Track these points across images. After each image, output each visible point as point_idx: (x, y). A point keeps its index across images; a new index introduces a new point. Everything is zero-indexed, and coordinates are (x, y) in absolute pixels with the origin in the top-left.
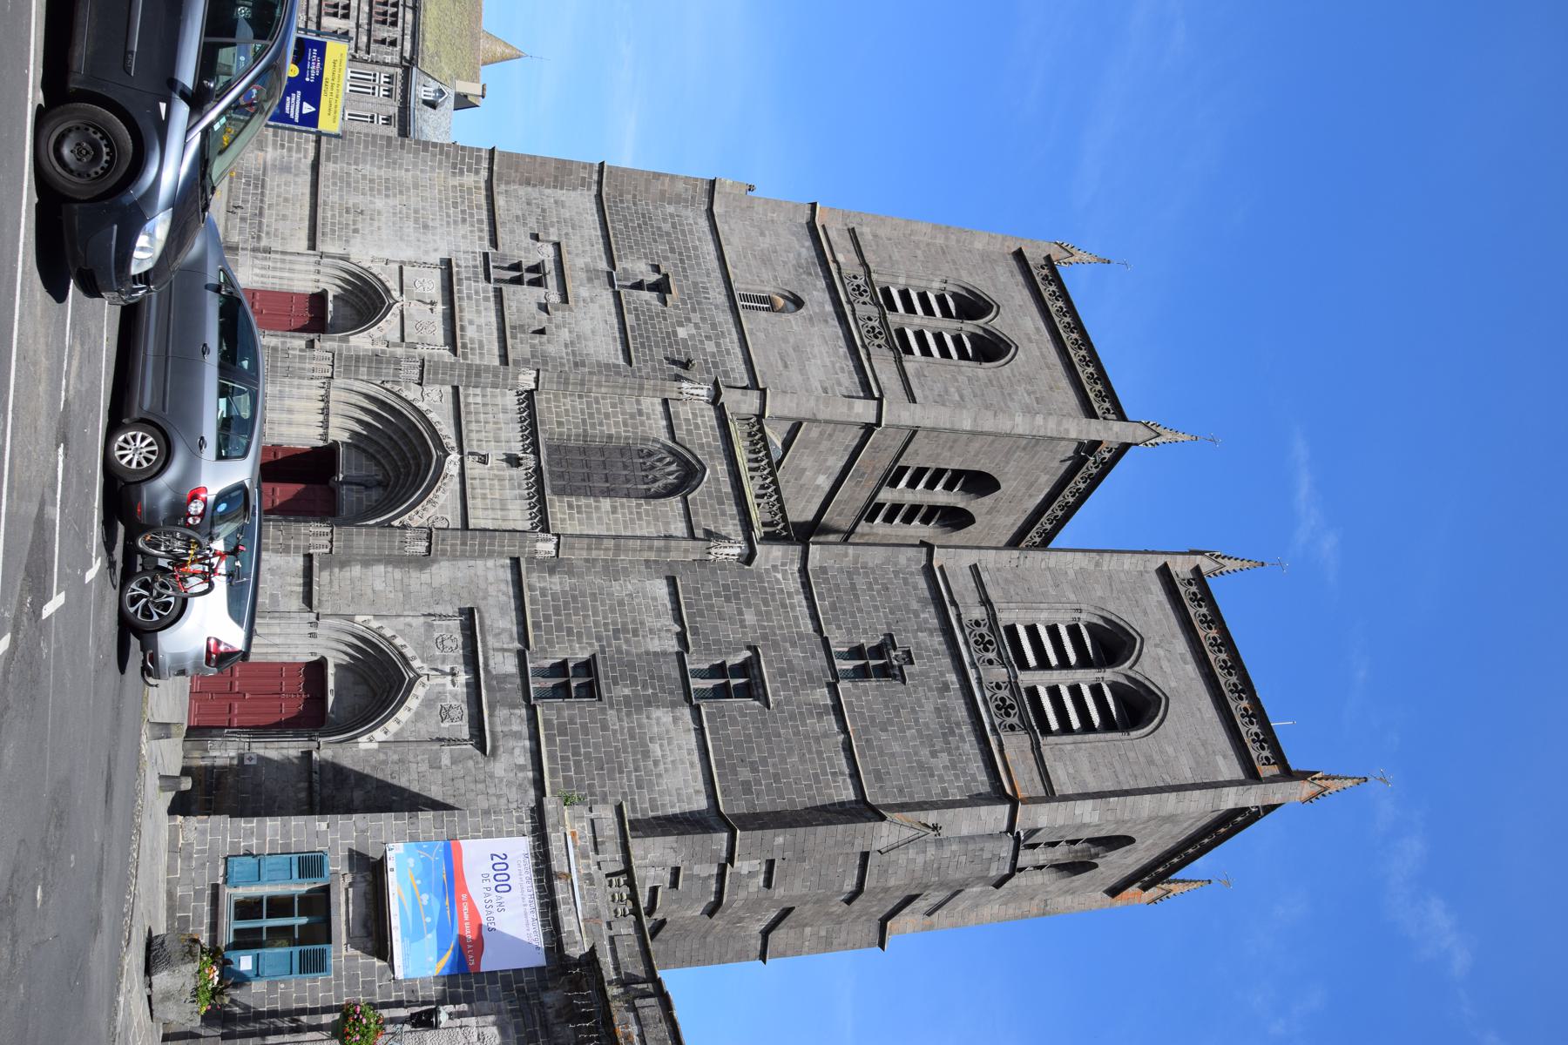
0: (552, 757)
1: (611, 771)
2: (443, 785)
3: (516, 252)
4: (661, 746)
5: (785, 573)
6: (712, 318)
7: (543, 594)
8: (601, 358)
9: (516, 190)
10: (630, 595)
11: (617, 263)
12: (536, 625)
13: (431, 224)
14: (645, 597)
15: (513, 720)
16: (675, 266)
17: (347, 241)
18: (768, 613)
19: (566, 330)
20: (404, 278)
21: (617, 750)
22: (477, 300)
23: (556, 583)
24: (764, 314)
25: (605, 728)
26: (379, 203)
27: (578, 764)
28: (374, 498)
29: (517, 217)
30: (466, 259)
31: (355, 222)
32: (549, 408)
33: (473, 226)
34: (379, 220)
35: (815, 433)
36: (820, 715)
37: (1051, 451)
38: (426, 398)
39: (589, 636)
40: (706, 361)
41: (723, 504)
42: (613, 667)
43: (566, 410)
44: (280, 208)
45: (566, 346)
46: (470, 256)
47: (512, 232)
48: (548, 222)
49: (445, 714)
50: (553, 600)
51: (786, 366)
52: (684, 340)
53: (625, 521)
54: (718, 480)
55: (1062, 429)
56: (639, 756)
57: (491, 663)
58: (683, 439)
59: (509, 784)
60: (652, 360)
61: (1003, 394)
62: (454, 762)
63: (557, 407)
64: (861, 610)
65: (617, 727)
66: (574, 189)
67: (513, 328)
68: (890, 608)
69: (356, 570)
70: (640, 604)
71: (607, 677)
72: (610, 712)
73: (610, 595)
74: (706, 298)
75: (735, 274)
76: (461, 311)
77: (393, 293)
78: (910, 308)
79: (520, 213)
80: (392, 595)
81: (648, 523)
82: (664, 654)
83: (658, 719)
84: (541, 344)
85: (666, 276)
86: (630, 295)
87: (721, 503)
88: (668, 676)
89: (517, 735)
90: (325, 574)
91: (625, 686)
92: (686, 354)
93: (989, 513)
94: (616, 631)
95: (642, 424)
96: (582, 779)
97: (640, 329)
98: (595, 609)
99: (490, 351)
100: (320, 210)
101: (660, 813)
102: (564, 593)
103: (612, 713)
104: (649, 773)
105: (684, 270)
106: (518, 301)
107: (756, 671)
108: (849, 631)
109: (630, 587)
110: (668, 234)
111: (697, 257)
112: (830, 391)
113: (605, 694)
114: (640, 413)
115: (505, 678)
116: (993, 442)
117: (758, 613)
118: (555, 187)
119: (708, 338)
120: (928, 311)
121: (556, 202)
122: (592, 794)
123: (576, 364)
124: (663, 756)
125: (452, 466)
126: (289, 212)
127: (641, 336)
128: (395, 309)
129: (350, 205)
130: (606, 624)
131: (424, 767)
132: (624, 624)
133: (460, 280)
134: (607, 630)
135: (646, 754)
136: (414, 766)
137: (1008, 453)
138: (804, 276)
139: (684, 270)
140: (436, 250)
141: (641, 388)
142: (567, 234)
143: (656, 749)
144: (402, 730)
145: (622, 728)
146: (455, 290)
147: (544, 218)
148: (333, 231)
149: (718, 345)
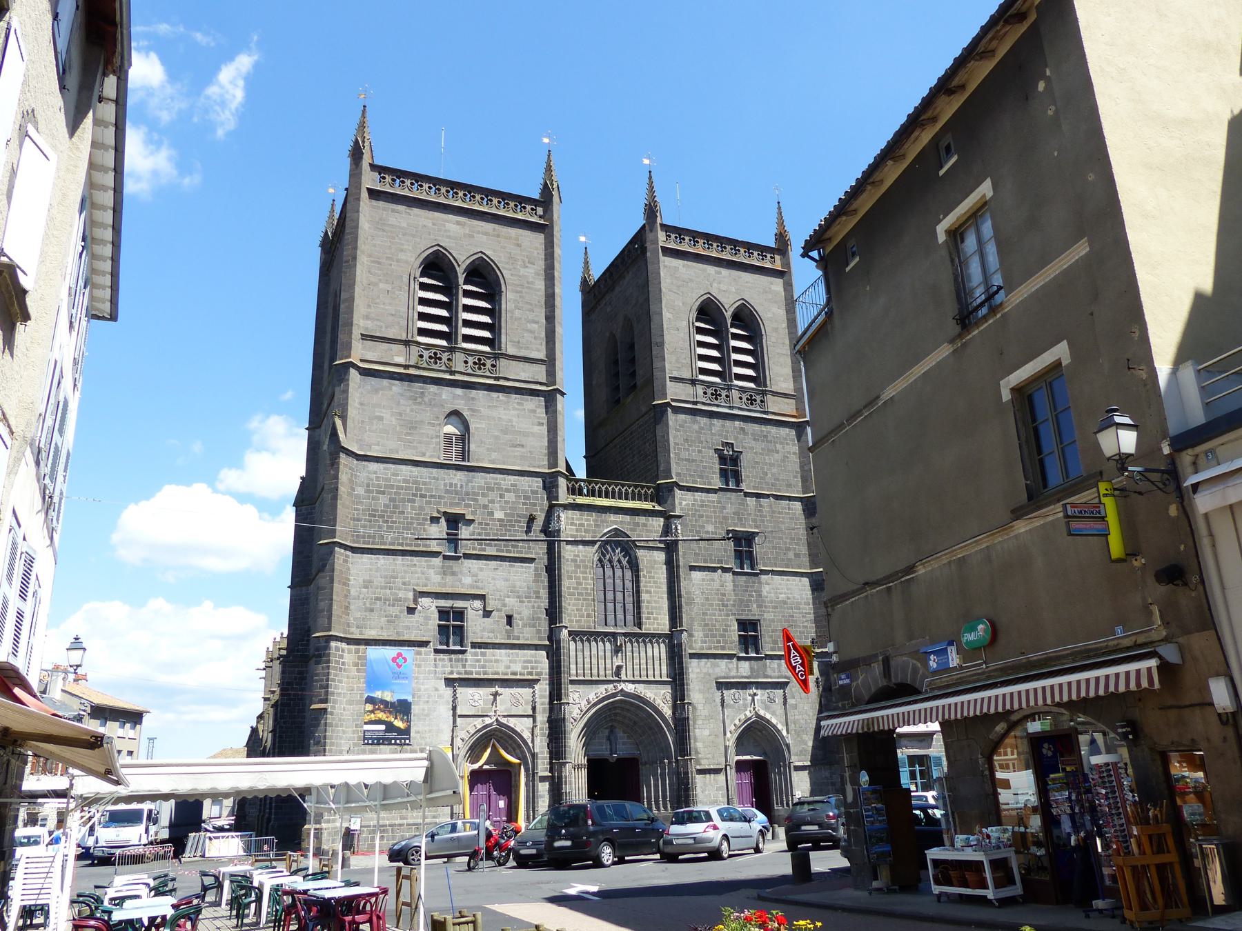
7: (705, 642)
9: (355, 619)
12: (723, 648)
16: (429, 503)
22: (485, 661)
25: (773, 621)
28: (622, 734)
32: (577, 621)
36: (761, 506)
38: (577, 701)
40: (524, 504)
47: (407, 628)
49: (772, 700)
51: (523, 446)
57: (745, 675)
64: (702, 462)
71: (748, 615)
72: (765, 617)
76: (497, 673)
79: (384, 619)
80: (712, 725)
81: (656, 573)
83: (767, 592)
85: (445, 513)
88: (745, 582)
92: (519, 516)
94: (723, 605)
95: (582, 561)
99: (532, 656)
101: (811, 601)
103: (766, 616)
105: (431, 496)
106: (484, 630)
110: (392, 500)
111: (415, 482)
113: (756, 618)
117: (708, 522)
119: (502, 496)
121: (366, 587)
123: (538, 597)
125: (629, 688)
128: (504, 721)
133: (466, 673)
135: (785, 602)
138: (426, 399)
139: (431, 496)
143: (782, 597)
146: (477, 677)
147: (385, 600)
149: (508, 491)
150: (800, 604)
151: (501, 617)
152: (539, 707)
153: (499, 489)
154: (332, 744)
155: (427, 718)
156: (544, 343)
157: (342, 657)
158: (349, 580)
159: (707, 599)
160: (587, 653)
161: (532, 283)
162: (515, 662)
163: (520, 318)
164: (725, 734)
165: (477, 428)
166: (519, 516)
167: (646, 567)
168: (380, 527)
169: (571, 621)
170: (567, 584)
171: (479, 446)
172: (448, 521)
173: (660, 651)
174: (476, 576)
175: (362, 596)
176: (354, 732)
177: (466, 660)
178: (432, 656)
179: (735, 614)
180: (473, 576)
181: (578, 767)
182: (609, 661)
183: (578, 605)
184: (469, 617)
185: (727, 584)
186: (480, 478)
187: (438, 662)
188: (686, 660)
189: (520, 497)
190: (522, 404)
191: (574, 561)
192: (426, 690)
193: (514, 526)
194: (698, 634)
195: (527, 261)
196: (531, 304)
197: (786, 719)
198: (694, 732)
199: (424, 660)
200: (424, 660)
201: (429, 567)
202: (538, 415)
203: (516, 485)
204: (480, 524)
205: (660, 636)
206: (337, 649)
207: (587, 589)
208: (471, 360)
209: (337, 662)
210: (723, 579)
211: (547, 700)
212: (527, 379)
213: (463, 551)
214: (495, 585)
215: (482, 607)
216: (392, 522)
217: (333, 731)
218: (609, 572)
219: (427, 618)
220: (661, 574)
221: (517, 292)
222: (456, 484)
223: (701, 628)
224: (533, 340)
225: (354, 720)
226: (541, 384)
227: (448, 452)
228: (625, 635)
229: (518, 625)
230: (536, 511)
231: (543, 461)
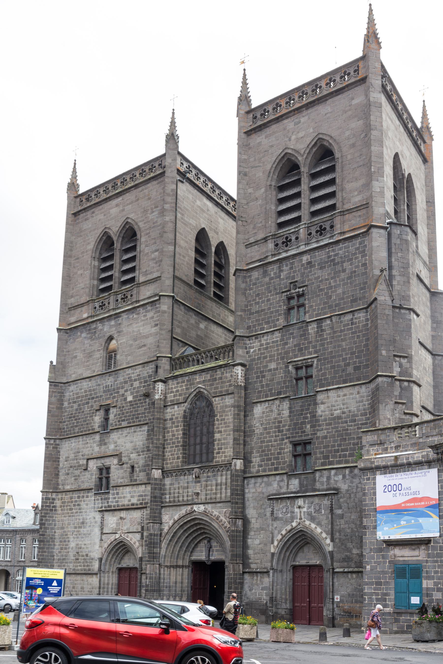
0: (339, 462)
1: (347, 434)
2: (351, 513)
3: (94, 480)
5: (250, 348)
6: (121, 383)
8: (145, 438)
10: (262, 424)
11: (96, 431)
12: (276, 469)
13: (81, 521)
14: (262, 417)
15: (321, 480)
16: (95, 402)
17: (92, 559)
18: (270, 356)
19: (131, 455)
21: (337, 431)
22: (118, 498)
23: (256, 460)
24: (118, 357)
25: (326, 437)
26: (72, 545)
27: (343, 450)
29: (75, 479)
30: (98, 504)
31: (83, 556)
32: (171, 463)
33: (81, 501)
34: (81, 545)
35: (178, 330)
37: (183, 199)
39: (282, 444)
40: (144, 386)
41: (216, 378)
42: (297, 433)
43: (171, 455)
44: (77, 590)
45: (139, 455)
46: (97, 502)
47: (83, 482)
48: (77, 465)
50: (264, 461)
51: (144, 346)
53: (226, 427)
54: (204, 381)
55: (171, 193)
56: (340, 421)
57: (294, 490)
58: (184, 398)
59: (352, 482)
60: (144, 413)
61: (154, 227)
62: (340, 508)
63: (170, 460)
65: (326, 431)
66: (59, 452)
67: (131, 481)
69: (250, 552)
70: (266, 420)
71: (301, 436)
72: (318, 435)
73: (261, 434)
74: (111, 386)
75: (98, 371)
76: (124, 505)
77: (117, 537)
78: (110, 278)
79: (73, 478)
81: (226, 415)
82: (290, 408)
83: (322, 411)
84: (139, 467)
86: (112, 424)
87: (215, 379)
88: (301, 406)
89: (329, 478)
90: (253, 566)
91: (306, 427)
92: (140, 397)
93: (217, 233)
94: (279, 431)
95: (177, 418)
96: (350, 448)
97: (129, 419)
98: (268, 442)
100: (78, 572)
102: (261, 456)
103: (319, 434)
104: (348, 416)
105: (97, 397)
106: (118, 478)
107: (300, 363)
108: (280, 315)
109: (257, 425)
110: (79, 405)
111: (90, 391)
112: (157, 323)
114: (171, 419)
115: (301, 484)
116: (180, 233)
117: (270, 361)
118: (59, 461)
119: (132, 385)
120: (110, 268)
121: (66, 461)
122: (357, 444)
123: (148, 450)
124: (340, 409)
126: (80, 586)
127: (132, 419)
129: (74, 558)
131: (342, 521)
132: (276, 427)
134: (278, 436)
135: (339, 418)
136: (342, 526)
137: (185, 224)
139: (97, 397)
140: (94, 518)
141: (159, 419)
142: (82, 456)
143: (337, 413)
144: (325, 531)
145: (326, 429)
148: (88, 566)
149: (135, 380)
150: (357, 416)
164: (272, 543)
167: (220, 412)
168: (73, 423)
174: (116, 443)
179: (289, 438)
197: (332, 528)
207: (178, 438)
210: (280, 408)
213: (111, 428)
219: (92, 475)
223: (258, 454)
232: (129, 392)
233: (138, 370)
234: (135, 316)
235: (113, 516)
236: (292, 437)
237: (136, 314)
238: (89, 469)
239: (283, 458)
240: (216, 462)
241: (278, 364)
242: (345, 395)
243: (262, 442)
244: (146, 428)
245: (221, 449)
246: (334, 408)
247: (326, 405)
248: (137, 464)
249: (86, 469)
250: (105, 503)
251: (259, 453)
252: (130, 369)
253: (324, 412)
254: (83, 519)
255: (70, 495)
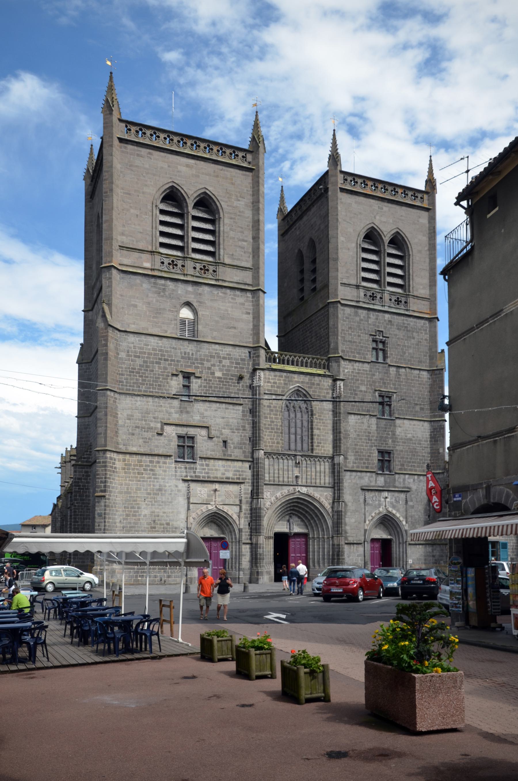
4: (408, 434)
6: (205, 355)
7: (355, 463)
10: (355, 431)
13: (158, 487)
14: (355, 426)
19: (223, 430)
20: (199, 502)
30: (181, 472)
32: (270, 446)
34: (158, 512)
39: (371, 450)
40: (236, 367)
42: (382, 444)
48: (146, 426)
51: (235, 328)
52: (223, 374)
67: (224, 455)
68: (359, 330)
71: (385, 447)
79: (141, 440)
82: (377, 424)
83: (399, 432)
85: (181, 372)
88: (385, 425)
91: (388, 441)
94: (369, 440)
99: (240, 467)
103: (397, 448)
106: (208, 450)
113: (391, 449)
119: (220, 362)
123: (244, 430)
130: (366, 443)
132: (366, 436)
133: (196, 476)
134: (368, 443)
140: (177, 486)
149: (224, 358)
151: (219, 442)
152: (244, 500)
153: (219, 357)
154: (109, 518)
155: (171, 504)
156: (251, 256)
157: (114, 464)
158: (117, 414)
159: (358, 435)
160: (276, 467)
161: (243, 212)
162: (228, 471)
163: (234, 238)
165: (202, 315)
166: (232, 376)
169: (266, 446)
170: (264, 422)
171: (205, 327)
172: (184, 377)
173: (325, 467)
175: (126, 425)
176: (123, 511)
177: (196, 469)
178: (173, 465)
179: (376, 446)
180: (201, 414)
181: (269, 538)
182: (290, 473)
183: (271, 435)
184: (198, 441)
185: (373, 426)
186: (206, 349)
187: (177, 469)
188: (343, 474)
189: (232, 363)
190: (235, 299)
191: (269, 407)
192: (169, 486)
193: (228, 382)
194: (351, 458)
195: (239, 195)
196: (242, 228)
198: (345, 520)
199: (169, 468)
200: (169, 468)
201: (171, 407)
202: (246, 307)
203: (230, 355)
204: (205, 380)
205: (325, 457)
206: (111, 458)
208: (198, 266)
209: (112, 467)
210: (370, 423)
211: (250, 496)
212: (239, 282)
214: (215, 421)
215: (207, 435)
216: (145, 377)
217: (110, 510)
218: (292, 415)
219: (170, 441)
220: (328, 418)
221: (231, 218)
222: (189, 353)
224: (243, 253)
225: (123, 504)
226: (248, 285)
227: (183, 330)
228: (302, 456)
229: (230, 447)
230: (244, 372)
231: (249, 338)
232: (217, 368)
233: (229, 349)
234: (220, 294)
235: (203, 487)
236: (379, 446)
237: (221, 292)
238: (165, 434)
239: (372, 460)
240: (316, 453)
241: (367, 388)
242: (414, 425)
243: (356, 445)
244: (241, 408)
245: (321, 443)
246: (407, 432)
247: (402, 429)
248: (232, 440)
249: (159, 434)
250: (190, 473)
251: (353, 452)
252: (217, 346)
253: (401, 433)
254: (160, 486)
255: (135, 458)
